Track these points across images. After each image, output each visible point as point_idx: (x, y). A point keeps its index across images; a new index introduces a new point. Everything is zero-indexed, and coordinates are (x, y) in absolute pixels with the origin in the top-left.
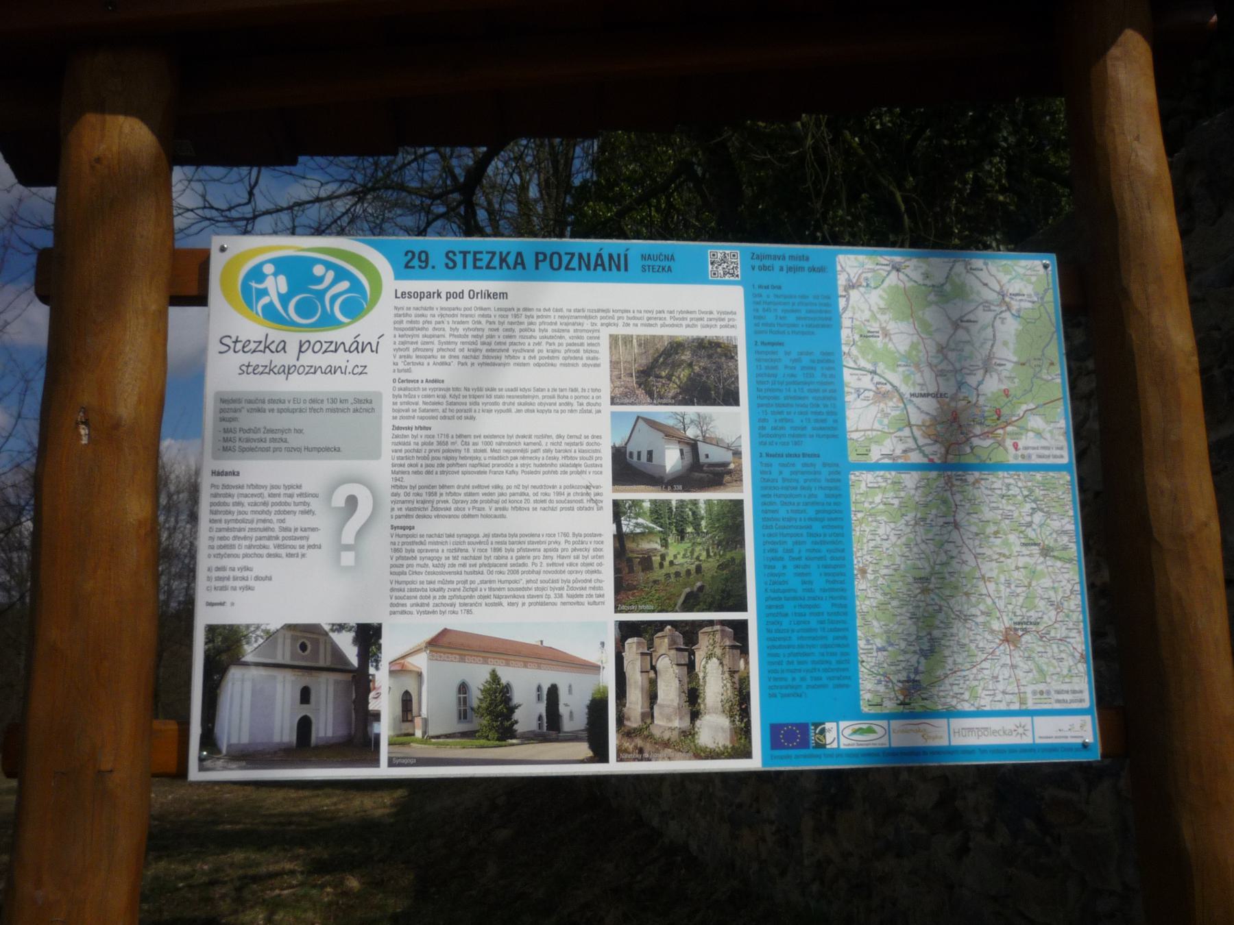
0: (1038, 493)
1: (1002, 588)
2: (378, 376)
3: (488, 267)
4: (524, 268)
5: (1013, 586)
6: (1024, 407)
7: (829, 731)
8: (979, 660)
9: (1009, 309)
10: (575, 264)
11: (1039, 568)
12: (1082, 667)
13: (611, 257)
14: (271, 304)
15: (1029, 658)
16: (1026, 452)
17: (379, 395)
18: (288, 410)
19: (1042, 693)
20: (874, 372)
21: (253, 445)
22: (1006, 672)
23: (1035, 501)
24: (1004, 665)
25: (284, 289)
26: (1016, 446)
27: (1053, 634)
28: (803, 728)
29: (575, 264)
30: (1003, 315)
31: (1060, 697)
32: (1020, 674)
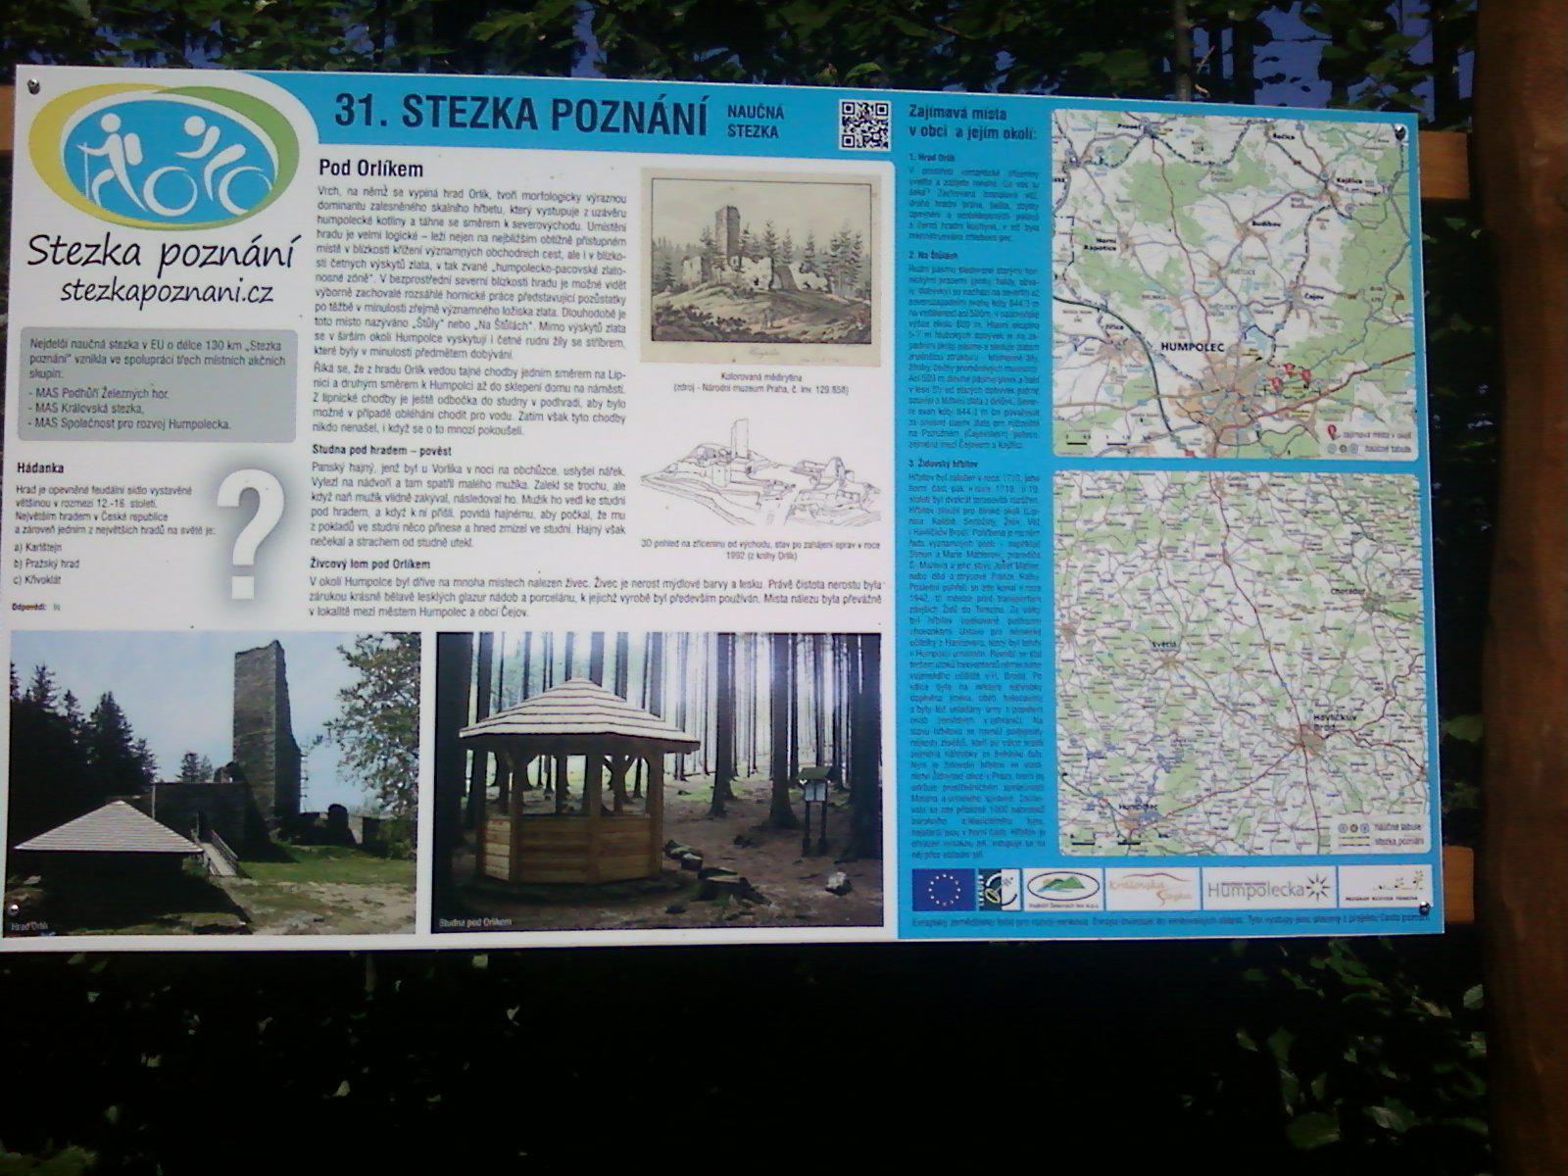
0: (1365, 508)
1: (1297, 660)
2: (291, 304)
3: (474, 124)
4: (534, 126)
6: (1350, 368)
7: (1008, 882)
8: (1254, 774)
10: (617, 120)
11: (1360, 629)
12: (1421, 789)
13: (677, 108)
14: (115, 182)
15: (1336, 773)
16: (1348, 442)
18: (142, 360)
19: (1354, 828)
21: (86, 416)
22: (1298, 794)
23: (1358, 522)
24: (1295, 784)
25: (136, 157)
27: (1376, 735)
28: (966, 876)
29: (617, 120)
30: (1323, 214)
31: (1384, 835)
32: (1320, 798)
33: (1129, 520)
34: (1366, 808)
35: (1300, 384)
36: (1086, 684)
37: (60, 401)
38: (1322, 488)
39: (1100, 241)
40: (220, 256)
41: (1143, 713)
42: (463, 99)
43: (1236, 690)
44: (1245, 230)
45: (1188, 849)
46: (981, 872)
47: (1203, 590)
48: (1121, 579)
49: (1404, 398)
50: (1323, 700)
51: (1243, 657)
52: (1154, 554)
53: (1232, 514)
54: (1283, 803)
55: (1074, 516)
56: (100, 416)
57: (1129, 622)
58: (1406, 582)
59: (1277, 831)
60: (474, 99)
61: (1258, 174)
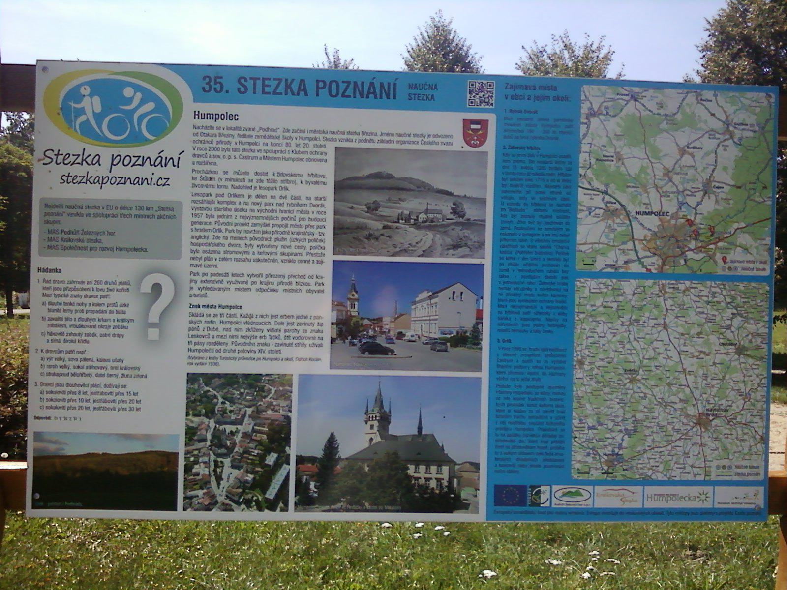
0: (739, 301)
1: (700, 380)
2: (180, 188)
3: (275, 93)
4: (306, 94)
5: (709, 380)
6: (736, 226)
7: (544, 492)
8: (674, 439)
9: (732, 137)
10: (350, 91)
13: (382, 85)
15: (716, 439)
16: (733, 265)
17: (180, 204)
18: (101, 215)
19: (724, 467)
20: (606, 193)
21: (73, 244)
22: (696, 449)
24: (694, 444)
25: (98, 109)
26: (724, 260)
27: (739, 420)
28: (522, 489)
29: (350, 91)
30: (726, 143)
31: (739, 471)
32: (707, 451)
33: (615, 305)
34: (731, 457)
35: (713, 235)
36: (589, 391)
37: (60, 236)
38: (718, 290)
39: (604, 156)
40: (143, 161)
41: (618, 406)
42: (269, 79)
43: (667, 395)
44: (682, 152)
45: (638, 477)
46: (530, 487)
47: (652, 343)
48: (610, 336)
49: (764, 242)
50: (712, 401)
51: (672, 378)
52: (627, 323)
53: (669, 303)
54: (688, 453)
55: (586, 302)
56: (79, 244)
57: (613, 359)
58: (759, 340)
59: (684, 468)
60: (275, 79)
61: (691, 122)
